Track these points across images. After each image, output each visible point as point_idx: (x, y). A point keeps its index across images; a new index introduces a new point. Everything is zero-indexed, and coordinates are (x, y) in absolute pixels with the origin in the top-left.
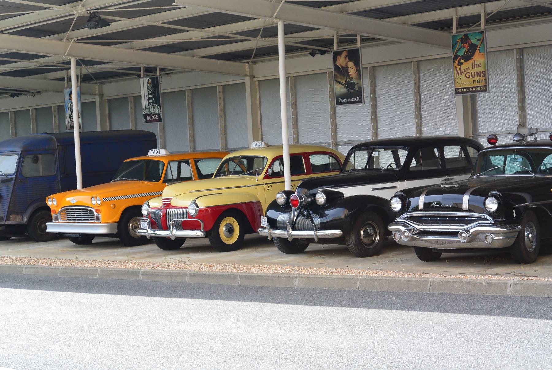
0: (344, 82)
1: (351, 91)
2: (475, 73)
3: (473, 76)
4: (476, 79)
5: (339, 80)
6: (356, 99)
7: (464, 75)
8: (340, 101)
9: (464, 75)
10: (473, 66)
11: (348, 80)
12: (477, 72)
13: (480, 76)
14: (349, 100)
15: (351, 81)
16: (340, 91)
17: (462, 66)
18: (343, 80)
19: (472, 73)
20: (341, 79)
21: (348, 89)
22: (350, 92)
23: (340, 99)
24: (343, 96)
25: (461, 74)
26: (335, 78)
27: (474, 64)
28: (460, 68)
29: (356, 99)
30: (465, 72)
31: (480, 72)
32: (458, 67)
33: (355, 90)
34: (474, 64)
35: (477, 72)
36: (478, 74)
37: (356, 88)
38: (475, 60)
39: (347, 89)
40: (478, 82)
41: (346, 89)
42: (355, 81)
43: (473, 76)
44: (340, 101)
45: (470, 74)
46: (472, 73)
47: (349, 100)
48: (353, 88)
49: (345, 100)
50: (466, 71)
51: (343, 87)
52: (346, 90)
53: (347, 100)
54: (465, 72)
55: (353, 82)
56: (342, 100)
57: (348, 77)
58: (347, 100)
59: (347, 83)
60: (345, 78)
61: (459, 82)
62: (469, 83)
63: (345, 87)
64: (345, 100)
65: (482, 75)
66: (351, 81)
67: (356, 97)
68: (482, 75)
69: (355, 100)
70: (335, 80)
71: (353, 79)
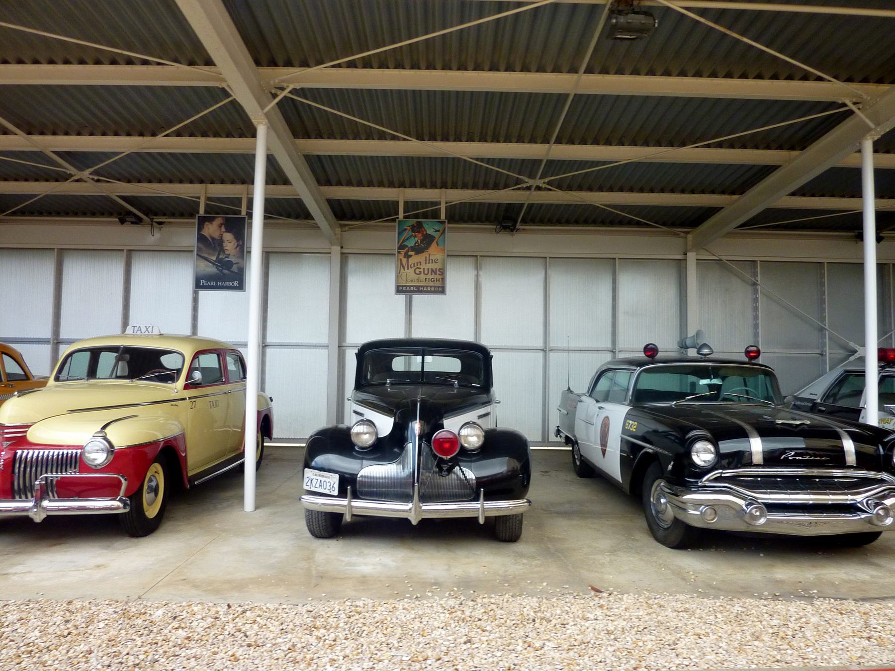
0: (214, 258)
1: (226, 272)
2: (428, 269)
3: (426, 272)
4: (430, 276)
5: (205, 255)
6: (233, 284)
7: (411, 271)
9: (411, 271)
10: (426, 260)
11: (220, 257)
12: (432, 269)
13: (435, 274)
15: (227, 259)
16: (204, 270)
17: (410, 259)
18: (213, 255)
19: (424, 269)
20: (209, 254)
22: (222, 273)
24: (209, 278)
25: (408, 269)
27: (428, 259)
28: (408, 261)
29: (233, 284)
30: (414, 266)
31: (436, 269)
32: (404, 260)
33: (232, 272)
34: (428, 259)
35: (432, 269)
36: (433, 271)
37: (235, 268)
38: (429, 255)
39: (218, 269)
40: (433, 280)
42: (232, 259)
43: (426, 272)
45: (422, 270)
46: (424, 269)
48: (229, 269)
50: (416, 265)
51: (211, 264)
52: (216, 269)
53: (216, 283)
54: (414, 266)
57: (221, 253)
58: (216, 283)
59: (219, 260)
60: (217, 253)
61: (404, 278)
62: (418, 280)
65: (438, 272)
66: (227, 259)
67: (232, 281)
68: (438, 272)
70: (197, 254)
71: (230, 257)
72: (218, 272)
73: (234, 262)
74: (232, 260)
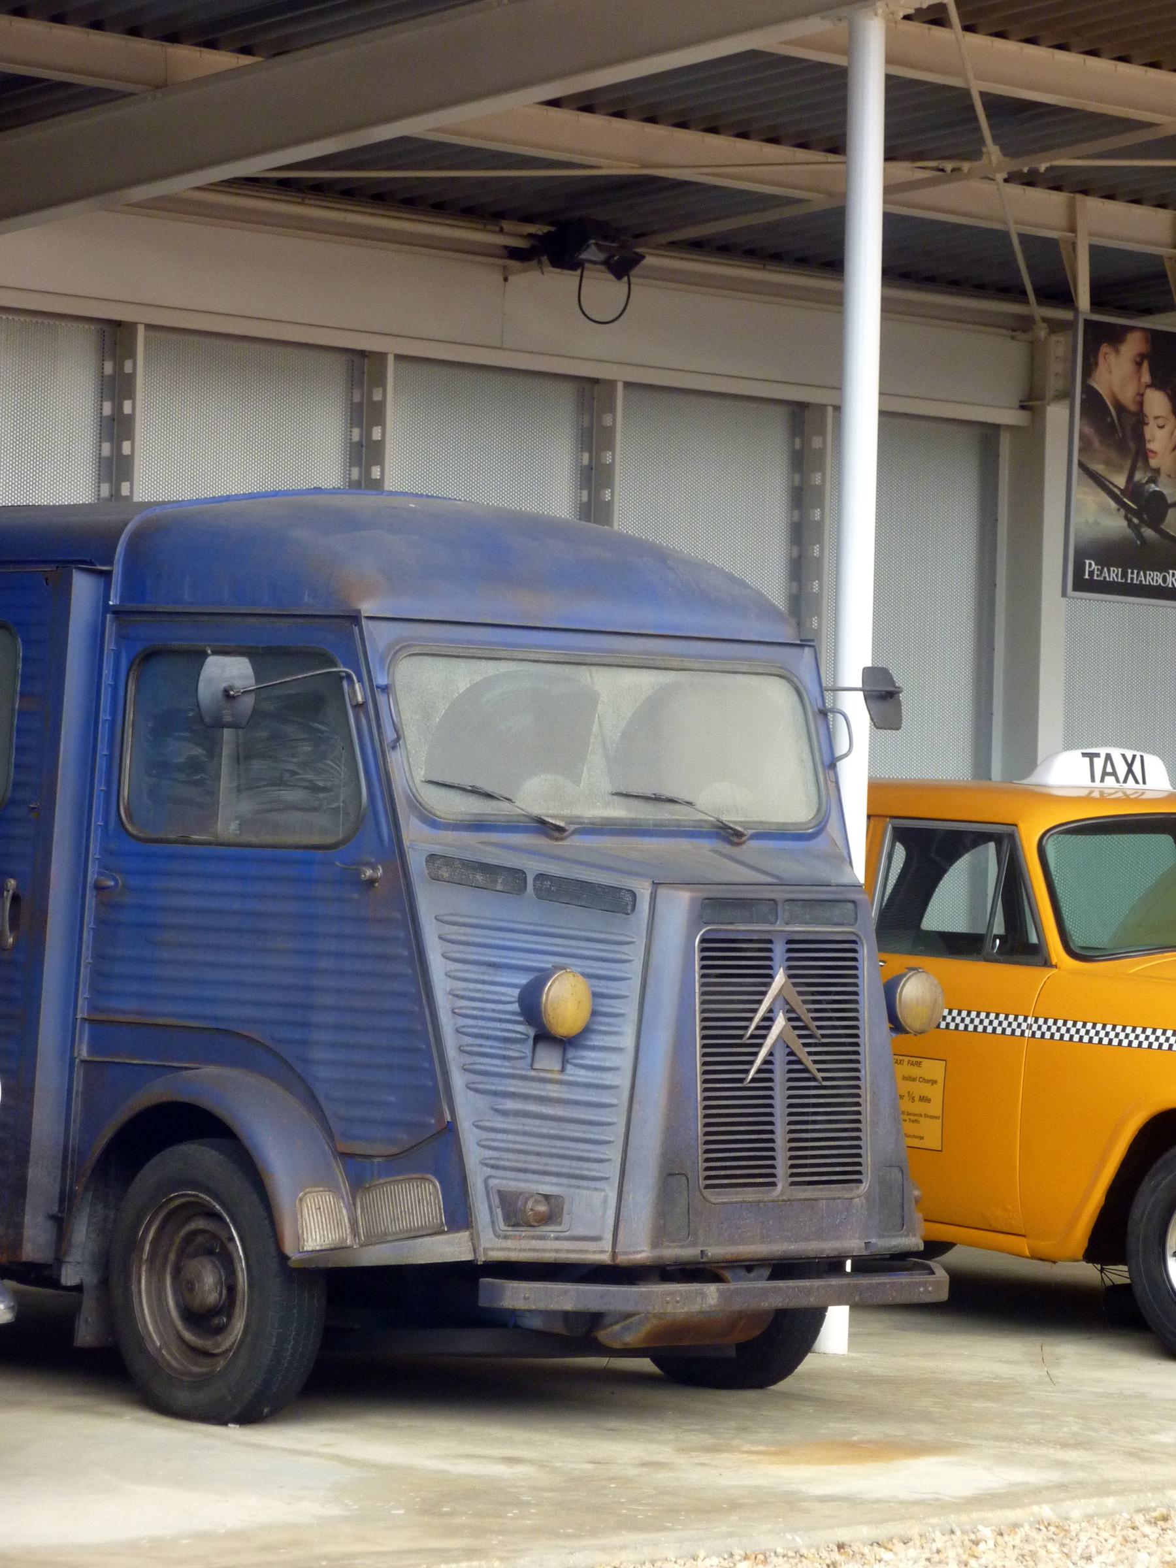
0: (1120, 481)
1: (1148, 532)
5: (1099, 468)
6: (1165, 579)
8: (1091, 573)
14: (1134, 577)
15: (1153, 487)
16: (1097, 523)
18: (1117, 468)
20: (1108, 463)
21: (1136, 521)
22: (1139, 535)
23: (1090, 565)
26: (1081, 450)
29: (1165, 579)
39: (1130, 524)
41: (1126, 518)
44: (1091, 573)
47: (1134, 577)
48: (1156, 520)
49: (1113, 575)
51: (1113, 505)
52: (1125, 523)
53: (1124, 575)
55: (1160, 496)
56: (1101, 571)
57: (1140, 464)
58: (1124, 575)
59: (1134, 490)
60: (1128, 464)
63: (1123, 512)
64: (1113, 575)
69: (1160, 581)
70: (1081, 464)
71: (1162, 479)
72: (1129, 531)
73: (1170, 500)
74: (1165, 492)
